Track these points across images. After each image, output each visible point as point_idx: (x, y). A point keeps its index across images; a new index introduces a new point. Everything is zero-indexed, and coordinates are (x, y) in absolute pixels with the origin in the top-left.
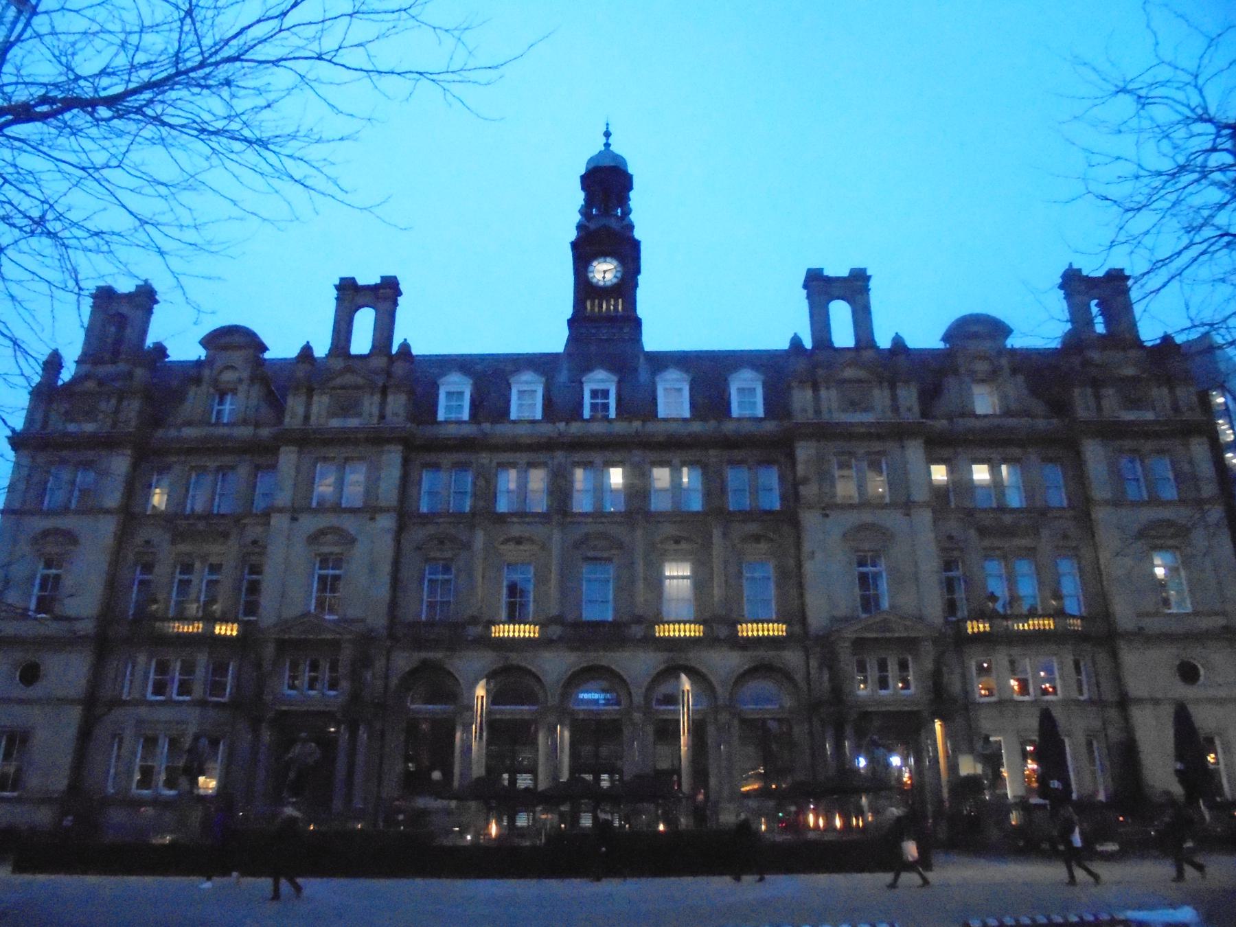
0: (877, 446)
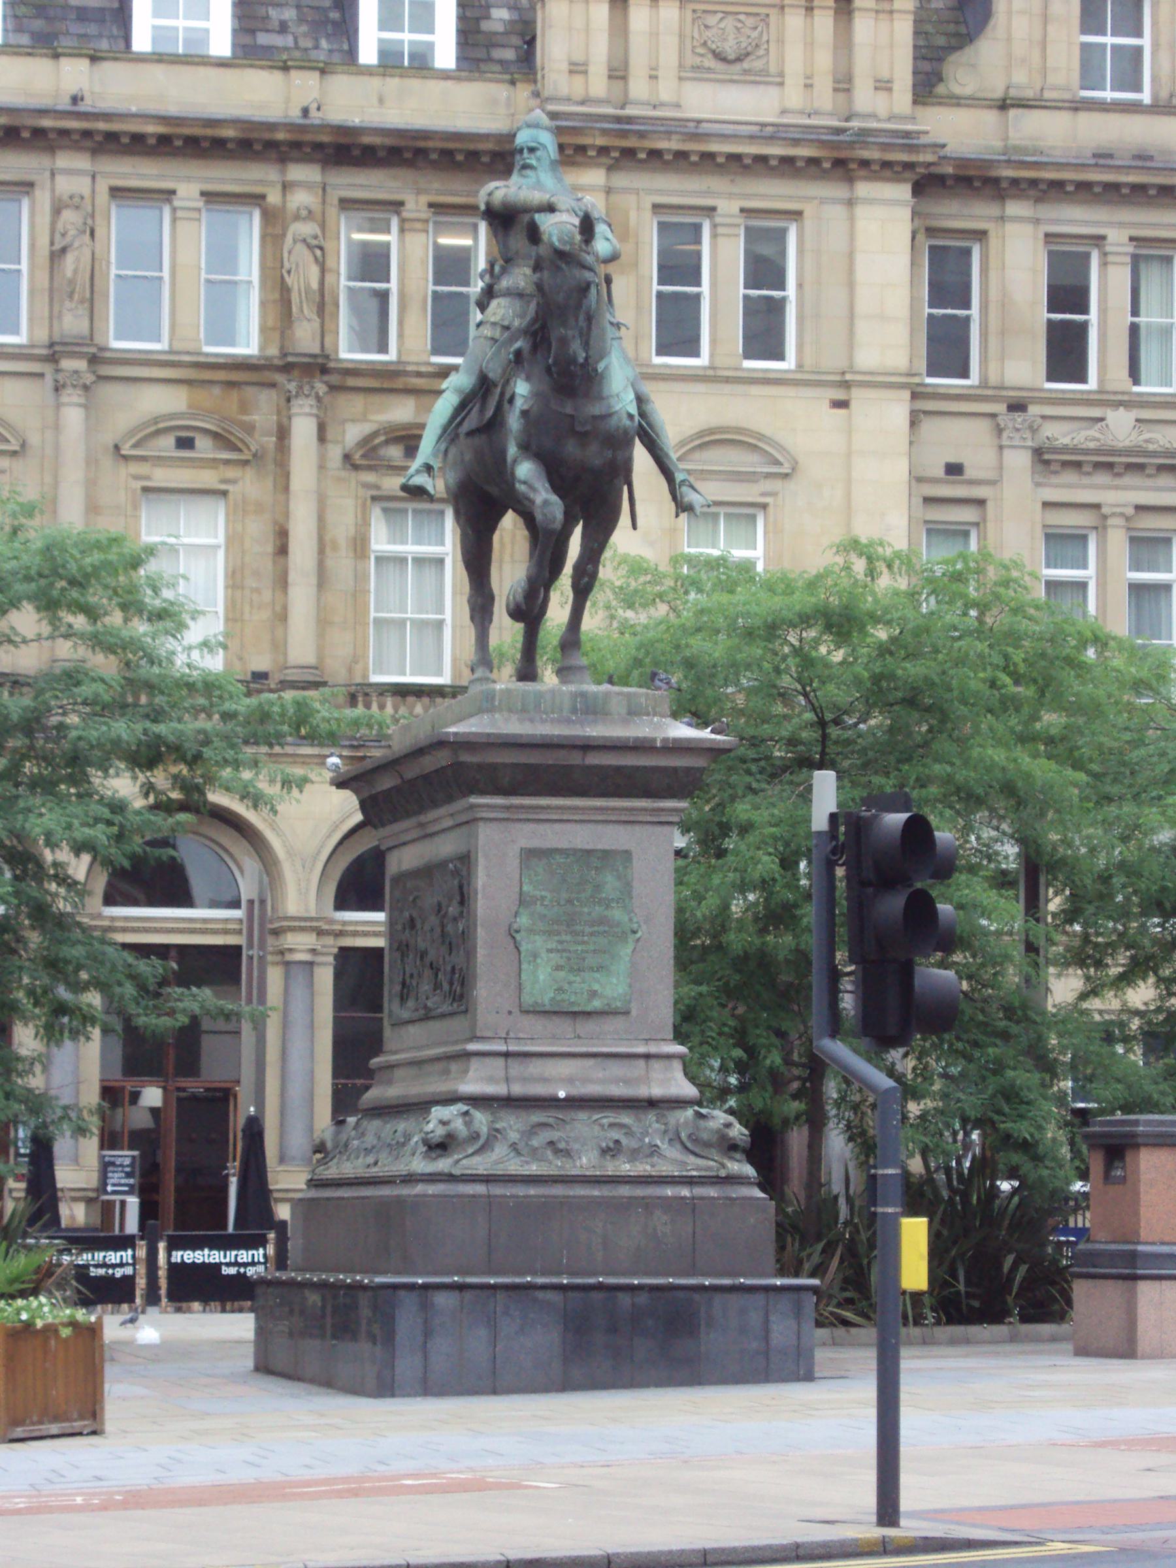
0: (772, 193)
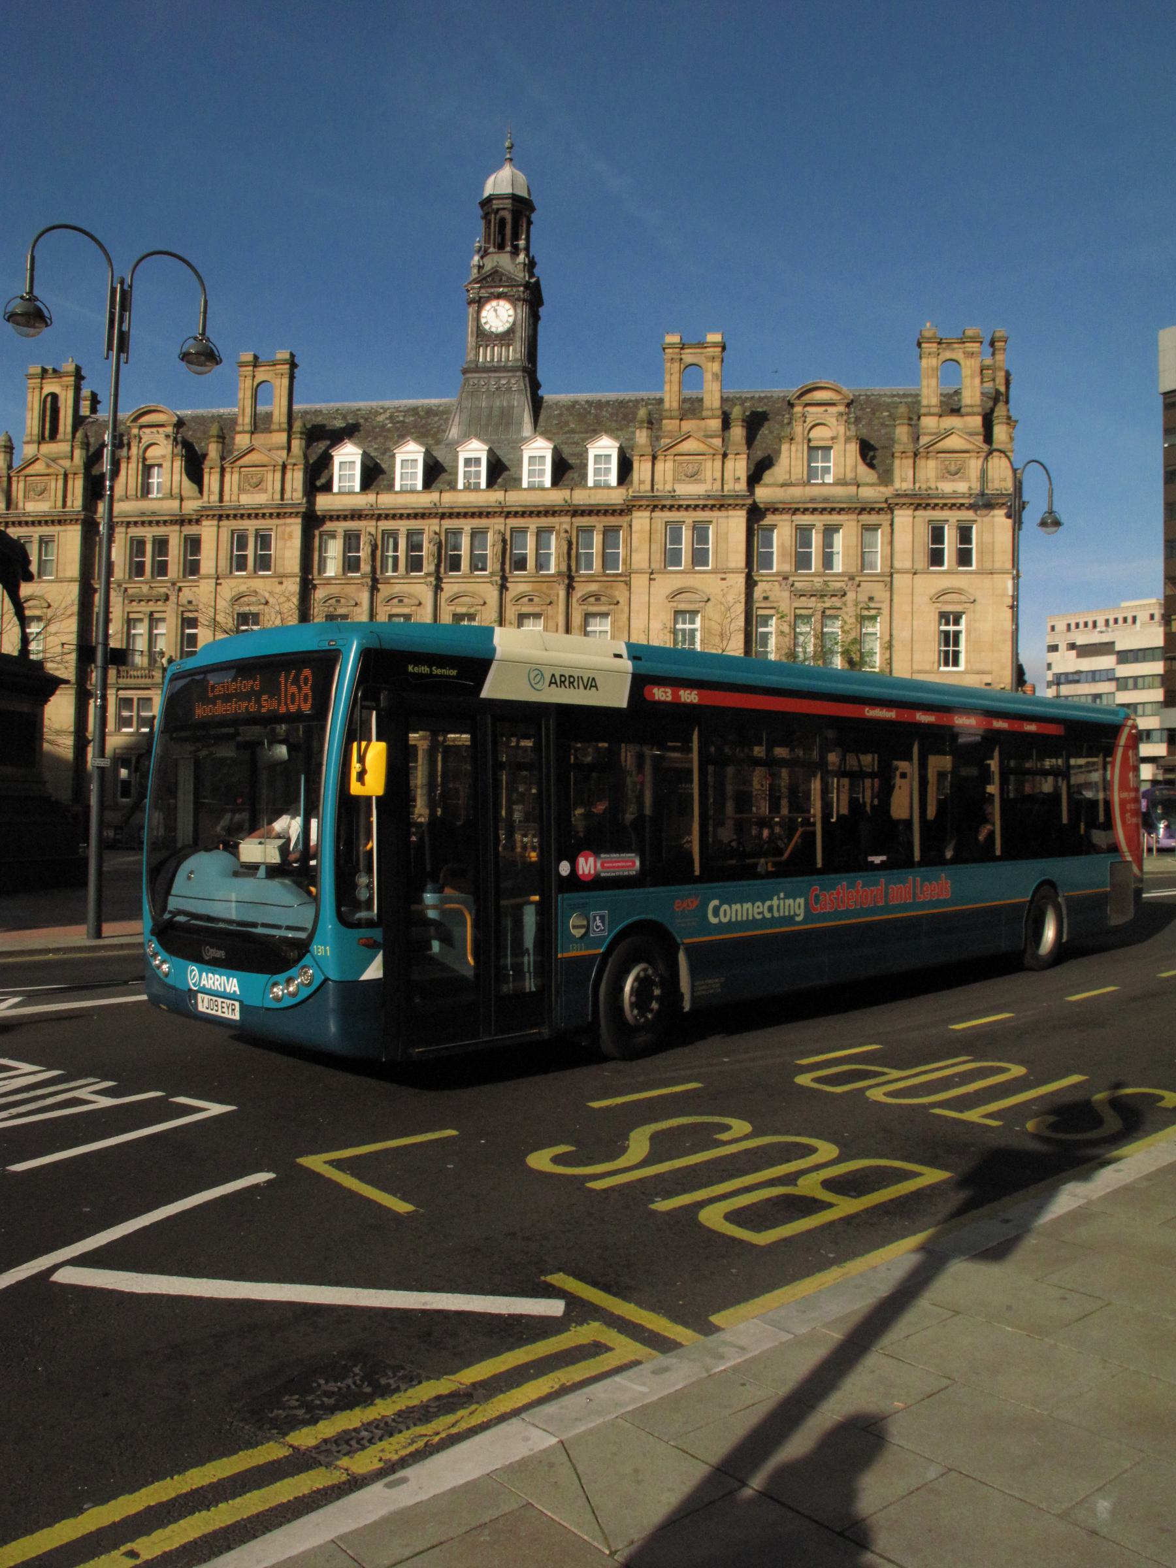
0: (701, 515)
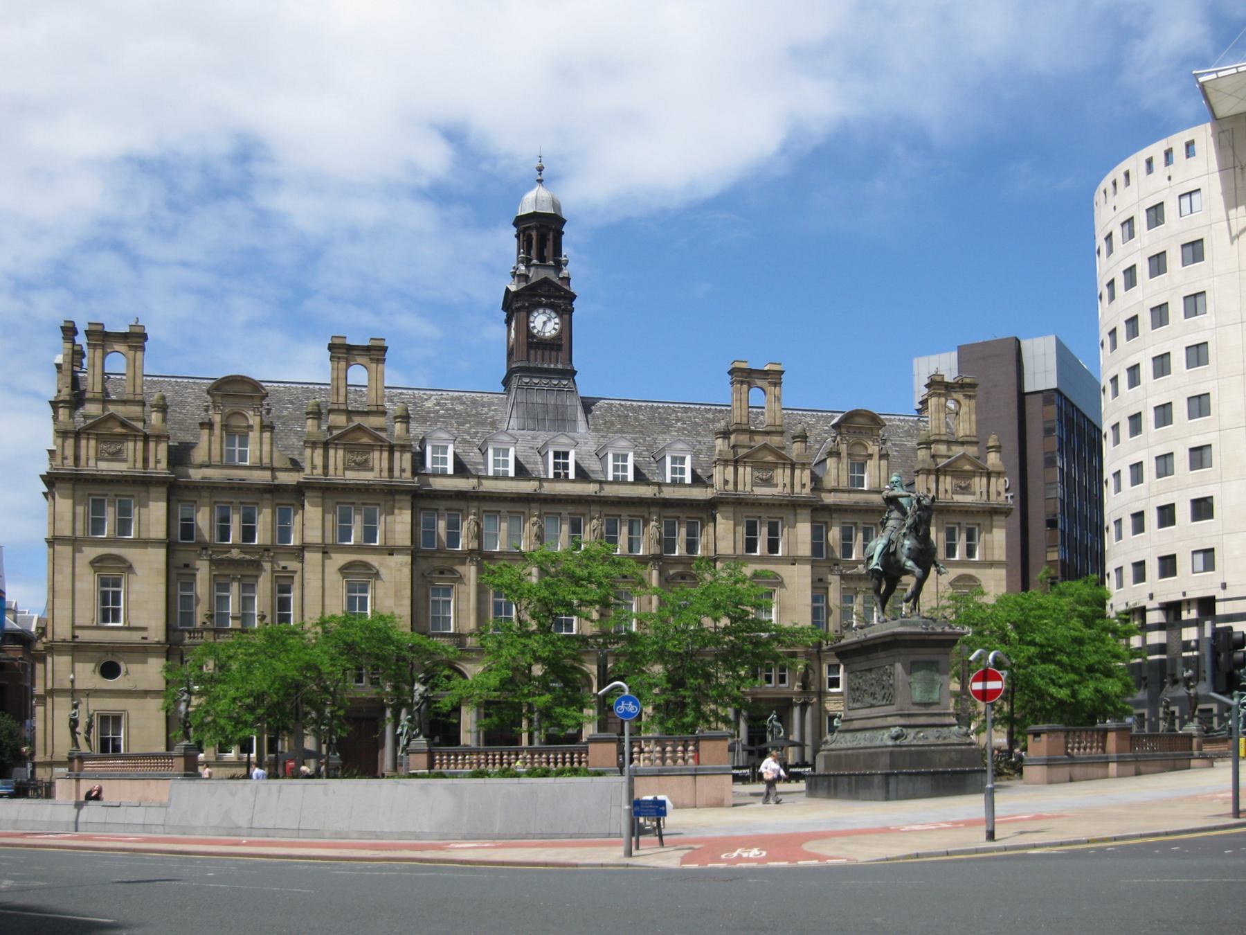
0: (775, 513)
